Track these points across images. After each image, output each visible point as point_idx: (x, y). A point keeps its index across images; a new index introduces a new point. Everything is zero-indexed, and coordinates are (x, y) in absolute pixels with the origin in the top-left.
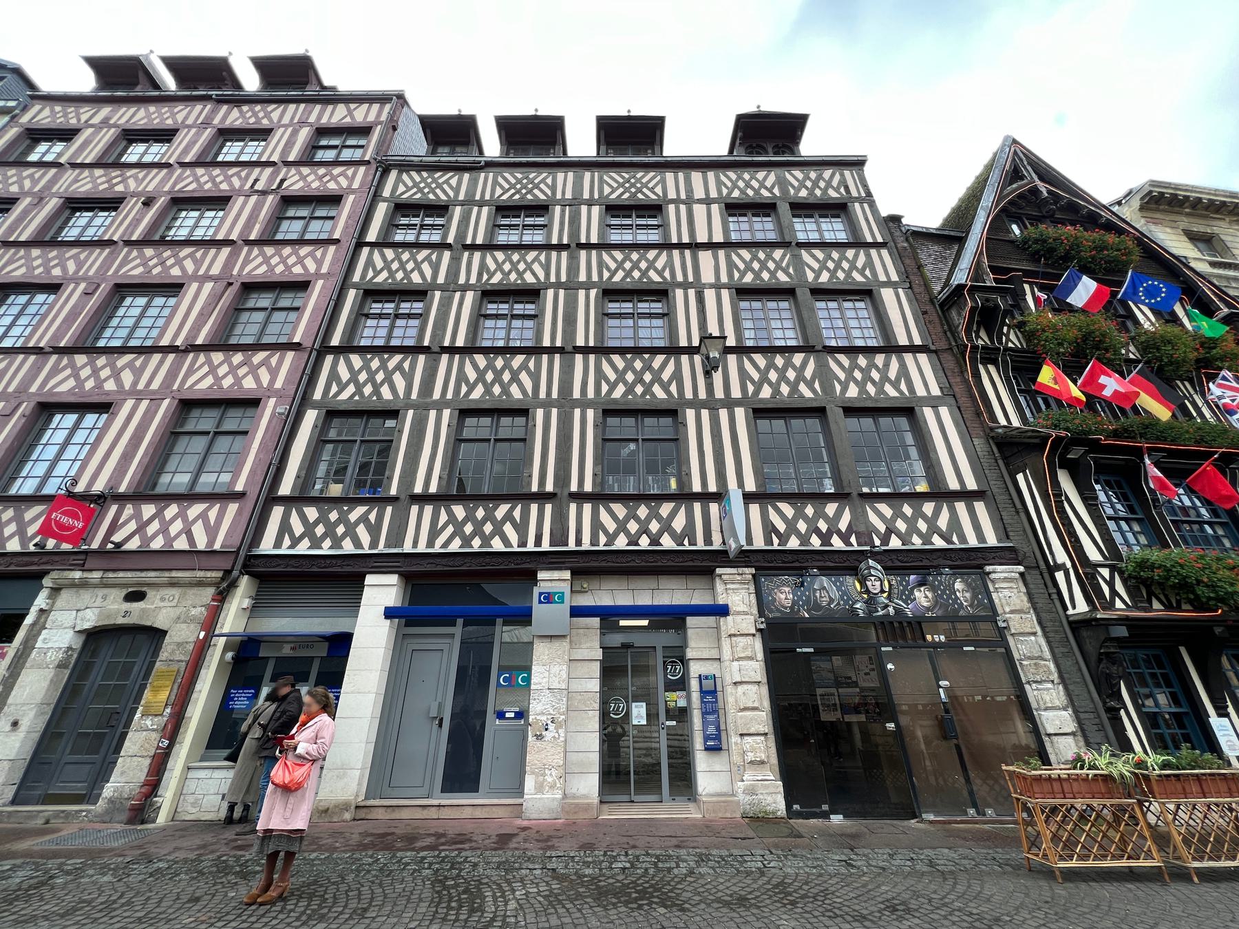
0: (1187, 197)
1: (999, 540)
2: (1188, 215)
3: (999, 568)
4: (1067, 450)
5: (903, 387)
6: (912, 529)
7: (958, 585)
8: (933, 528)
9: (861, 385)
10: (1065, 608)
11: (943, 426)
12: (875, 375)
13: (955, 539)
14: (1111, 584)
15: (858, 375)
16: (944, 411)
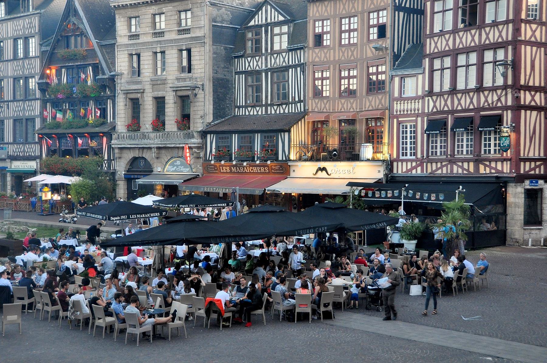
2: (130, 8)
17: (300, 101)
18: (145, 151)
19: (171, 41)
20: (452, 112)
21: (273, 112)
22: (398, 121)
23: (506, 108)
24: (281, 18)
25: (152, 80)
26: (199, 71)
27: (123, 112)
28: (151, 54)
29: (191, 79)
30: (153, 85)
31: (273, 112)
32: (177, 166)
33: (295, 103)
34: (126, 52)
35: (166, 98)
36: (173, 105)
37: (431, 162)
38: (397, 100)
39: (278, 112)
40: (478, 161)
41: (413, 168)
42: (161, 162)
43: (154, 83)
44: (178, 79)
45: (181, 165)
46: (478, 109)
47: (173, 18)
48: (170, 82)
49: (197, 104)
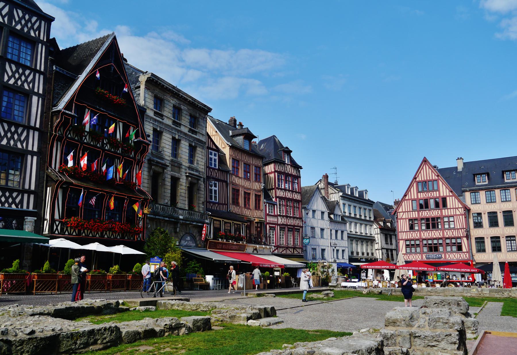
0: (160, 83)
1: (33, 209)
2: (159, 89)
3: (29, 218)
4: (63, 184)
5: (24, 145)
6: (7, 201)
7: (14, 222)
8: (14, 202)
9: (9, 140)
10: (43, 232)
11: (32, 164)
12: (16, 137)
13: (19, 207)
14: (57, 226)
15: (9, 135)
16: (35, 158)
17: (225, 204)
18: (166, 224)
19: (185, 134)
20: (287, 225)
21: (210, 208)
22: (269, 227)
23: (300, 227)
24: (214, 147)
25: (172, 161)
26: (202, 167)
27: (146, 181)
28: (171, 137)
29: (197, 171)
30: (172, 165)
31: (210, 208)
32: (188, 241)
33: (223, 204)
34: (152, 125)
35: (181, 180)
36: (184, 187)
37: (281, 247)
38: (269, 215)
39: (213, 208)
40: (294, 248)
41: (275, 250)
42: (178, 237)
43: (173, 164)
44: (189, 168)
45: (190, 240)
46: (294, 226)
47: (187, 117)
48: (183, 167)
49: (200, 192)
